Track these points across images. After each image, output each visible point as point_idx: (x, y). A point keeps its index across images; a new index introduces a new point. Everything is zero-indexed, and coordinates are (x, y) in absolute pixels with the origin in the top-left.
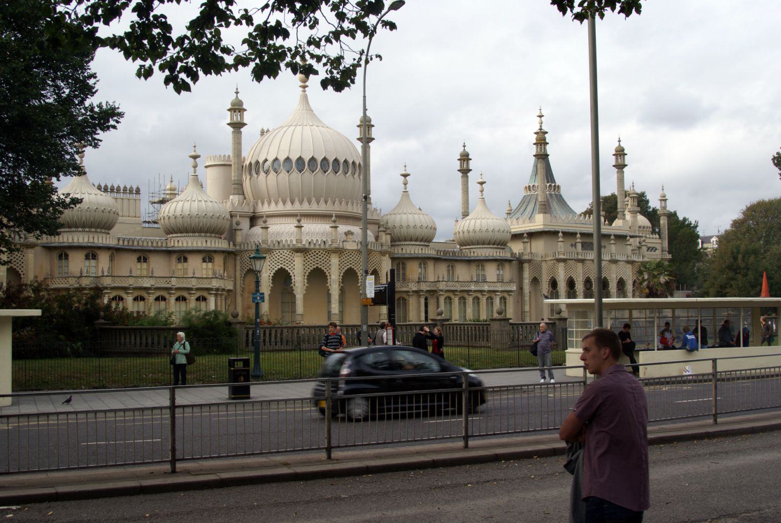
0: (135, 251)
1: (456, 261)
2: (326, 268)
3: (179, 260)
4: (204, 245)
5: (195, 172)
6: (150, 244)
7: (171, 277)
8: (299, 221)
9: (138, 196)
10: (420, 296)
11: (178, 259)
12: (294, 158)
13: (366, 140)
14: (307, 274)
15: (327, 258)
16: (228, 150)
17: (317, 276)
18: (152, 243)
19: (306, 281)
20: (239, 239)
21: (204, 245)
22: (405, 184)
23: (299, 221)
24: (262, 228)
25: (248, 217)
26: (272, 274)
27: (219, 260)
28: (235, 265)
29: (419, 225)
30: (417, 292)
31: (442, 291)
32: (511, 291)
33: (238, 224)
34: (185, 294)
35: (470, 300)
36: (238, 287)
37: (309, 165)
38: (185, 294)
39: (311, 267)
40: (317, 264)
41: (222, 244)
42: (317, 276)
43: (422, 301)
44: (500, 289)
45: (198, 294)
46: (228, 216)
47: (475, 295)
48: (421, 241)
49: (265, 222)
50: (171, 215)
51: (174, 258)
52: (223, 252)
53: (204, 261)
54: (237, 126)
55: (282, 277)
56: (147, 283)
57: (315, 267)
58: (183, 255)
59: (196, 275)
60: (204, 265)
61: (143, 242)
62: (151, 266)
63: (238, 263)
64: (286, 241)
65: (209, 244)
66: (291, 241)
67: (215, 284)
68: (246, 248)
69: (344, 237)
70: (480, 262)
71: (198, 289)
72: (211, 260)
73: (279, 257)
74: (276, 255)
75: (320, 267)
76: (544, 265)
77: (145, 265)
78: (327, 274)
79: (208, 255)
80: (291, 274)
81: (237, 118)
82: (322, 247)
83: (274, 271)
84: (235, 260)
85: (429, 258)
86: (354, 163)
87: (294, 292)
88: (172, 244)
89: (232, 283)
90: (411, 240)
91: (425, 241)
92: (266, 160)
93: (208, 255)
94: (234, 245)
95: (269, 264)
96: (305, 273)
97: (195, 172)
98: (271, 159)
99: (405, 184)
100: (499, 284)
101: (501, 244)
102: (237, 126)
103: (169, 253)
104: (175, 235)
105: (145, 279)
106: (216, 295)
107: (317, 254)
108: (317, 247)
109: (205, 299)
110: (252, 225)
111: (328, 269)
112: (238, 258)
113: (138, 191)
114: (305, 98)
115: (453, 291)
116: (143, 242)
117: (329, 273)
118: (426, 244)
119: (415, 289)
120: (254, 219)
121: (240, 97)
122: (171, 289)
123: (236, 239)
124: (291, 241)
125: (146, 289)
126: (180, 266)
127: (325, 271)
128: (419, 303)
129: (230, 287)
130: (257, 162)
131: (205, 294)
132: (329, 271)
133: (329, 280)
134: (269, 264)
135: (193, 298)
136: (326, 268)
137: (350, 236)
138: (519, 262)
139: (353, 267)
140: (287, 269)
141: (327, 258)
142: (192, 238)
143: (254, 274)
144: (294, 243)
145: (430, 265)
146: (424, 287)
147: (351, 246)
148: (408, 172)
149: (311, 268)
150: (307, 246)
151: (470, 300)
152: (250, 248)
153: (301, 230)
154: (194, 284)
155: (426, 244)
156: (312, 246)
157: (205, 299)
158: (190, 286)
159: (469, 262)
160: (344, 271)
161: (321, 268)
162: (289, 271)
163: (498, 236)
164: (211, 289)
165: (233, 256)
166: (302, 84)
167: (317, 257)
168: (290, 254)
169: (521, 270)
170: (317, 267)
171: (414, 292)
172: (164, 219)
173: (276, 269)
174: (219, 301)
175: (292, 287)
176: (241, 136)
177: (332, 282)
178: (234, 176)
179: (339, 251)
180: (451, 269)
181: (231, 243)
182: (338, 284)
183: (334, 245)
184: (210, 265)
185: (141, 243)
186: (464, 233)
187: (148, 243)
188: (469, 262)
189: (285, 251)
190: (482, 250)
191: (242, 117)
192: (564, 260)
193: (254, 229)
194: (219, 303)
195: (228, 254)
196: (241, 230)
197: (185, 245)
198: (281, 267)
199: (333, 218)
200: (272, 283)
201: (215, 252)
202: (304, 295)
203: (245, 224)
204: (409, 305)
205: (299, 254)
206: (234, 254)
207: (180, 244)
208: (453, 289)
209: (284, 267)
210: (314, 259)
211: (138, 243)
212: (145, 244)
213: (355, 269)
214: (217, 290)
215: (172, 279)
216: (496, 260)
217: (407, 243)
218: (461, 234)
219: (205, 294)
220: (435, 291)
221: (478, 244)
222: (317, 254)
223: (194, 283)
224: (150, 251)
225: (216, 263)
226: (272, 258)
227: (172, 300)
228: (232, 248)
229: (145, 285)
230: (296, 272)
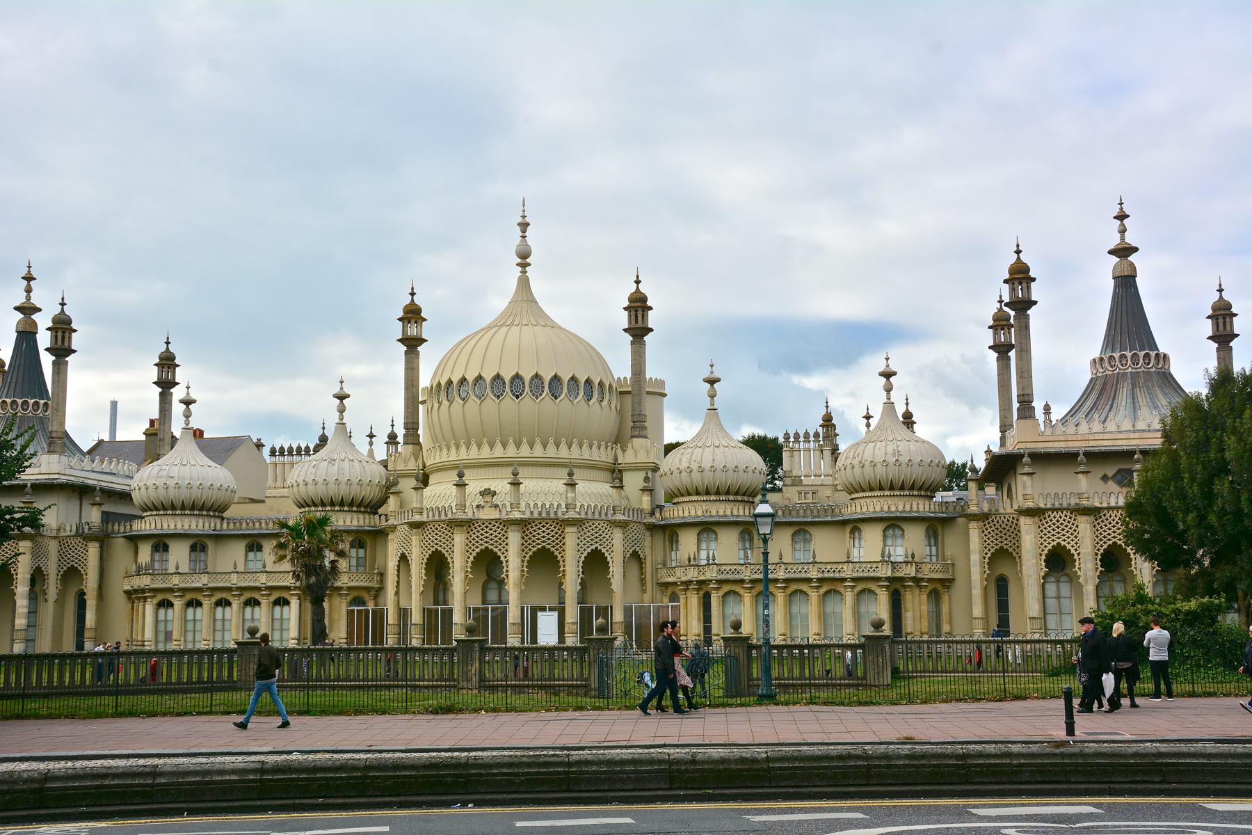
0: (244, 536)
13: (639, 331)
18: (267, 524)
22: (712, 396)
29: (731, 466)
47: (793, 587)
54: (412, 344)
69: (479, 500)
70: (854, 526)
81: (412, 331)
99: (712, 396)
101: (927, 490)
102: (412, 344)
109: (287, 603)
114: (524, 282)
119: (684, 579)
121: (417, 300)
125: (199, 590)
131: (285, 595)
137: (488, 498)
146: (692, 574)
148: (716, 375)
157: (287, 603)
158: (258, 584)
160: (474, 554)
163: (919, 474)
166: (519, 260)
171: (683, 583)
176: (418, 357)
190: (890, 501)
217: (685, 499)
227: (236, 604)
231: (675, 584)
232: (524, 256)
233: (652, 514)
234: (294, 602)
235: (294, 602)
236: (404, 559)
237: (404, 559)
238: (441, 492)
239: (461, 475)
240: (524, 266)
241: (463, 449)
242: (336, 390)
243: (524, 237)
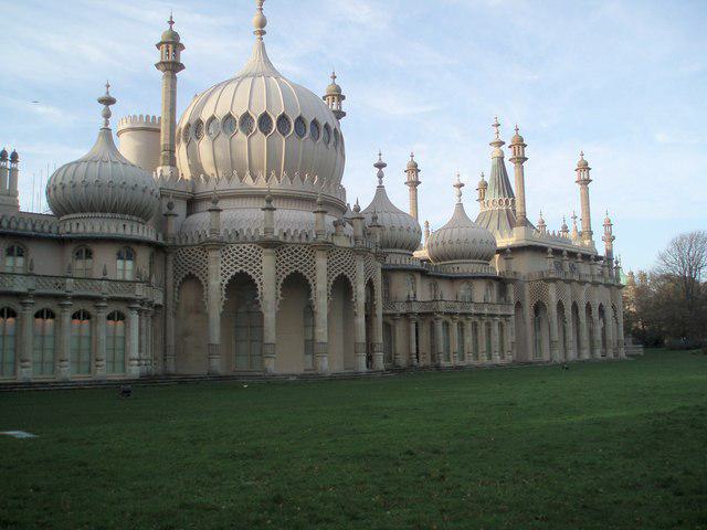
1: (440, 277)
3: (78, 255)
4: (121, 231)
5: (107, 125)
6: (30, 227)
7: (67, 277)
8: (269, 201)
9: (14, 165)
10: (409, 321)
11: (77, 254)
12: (256, 115)
14: (281, 281)
15: (311, 257)
16: (157, 110)
17: (296, 285)
19: (280, 292)
20: (173, 228)
23: (269, 201)
24: (210, 210)
25: (184, 199)
26: (226, 282)
27: (143, 256)
28: (166, 269)
30: (406, 315)
31: (439, 313)
32: (510, 316)
33: (170, 206)
34: (88, 307)
35: (469, 326)
36: (170, 303)
37: (278, 125)
38: (88, 307)
41: (147, 232)
42: (296, 285)
43: (413, 326)
44: (500, 312)
45: (113, 308)
46: (157, 191)
48: (401, 248)
49: (215, 202)
50: (67, 182)
51: (70, 250)
52: (149, 244)
53: (120, 257)
54: (172, 67)
55: (242, 286)
56: (20, 286)
58: (84, 246)
59: (108, 277)
60: (120, 262)
61: (17, 223)
62: (29, 259)
63: (170, 267)
64: (249, 230)
65: (128, 232)
66: (257, 230)
67: (140, 292)
68: (184, 243)
71: (112, 300)
72: (130, 256)
74: (233, 252)
76: (527, 286)
77: (20, 261)
78: (311, 281)
79: (127, 247)
80: (257, 281)
82: (304, 240)
83: (229, 277)
84: (166, 259)
85: (417, 271)
87: (262, 309)
88: (68, 230)
89: (161, 295)
90: (395, 247)
92: (213, 118)
93: (127, 247)
94: (165, 239)
95: (221, 265)
97: (107, 125)
98: (220, 114)
99: (380, 176)
100: (499, 307)
103: (61, 242)
104: (72, 216)
105: (18, 277)
106: (140, 312)
107: (296, 251)
108: (297, 240)
110: (190, 211)
112: (171, 258)
113: (14, 157)
115: (451, 314)
116: (17, 223)
118: (408, 252)
119: (404, 311)
120: (192, 203)
121: (175, 28)
122: (64, 297)
123: (167, 229)
124: (257, 230)
125: (18, 295)
126: (79, 264)
127: (308, 277)
128: (409, 330)
129: (159, 301)
130: (199, 122)
133: (313, 292)
134: (221, 265)
135: (103, 314)
138: (502, 283)
140: (250, 273)
141: (311, 257)
142: (101, 221)
143: (193, 280)
144: (262, 233)
145: (418, 277)
147: (341, 242)
148: (384, 161)
149: (288, 273)
150: (281, 238)
151: (469, 326)
152: (189, 242)
153: (272, 214)
154: (105, 290)
155: (408, 252)
156: (289, 240)
157: (121, 317)
159: (452, 279)
162: (254, 277)
164: (134, 301)
165: (162, 255)
168: (255, 251)
169: (503, 291)
171: (402, 315)
172: (55, 189)
173: (233, 273)
174: (144, 321)
175: (258, 302)
177: (318, 294)
178: (163, 139)
179: (328, 247)
180: (434, 287)
181: (160, 235)
182: (326, 297)
183: (321, 239)
184: (129, 264)
185: (13, 224)
187: (26, 225)
188: (452, 279)
189: (247, 246)
191: (176, 54)
192: (554, 280)
193: (191, 217)
194: (144, 325)
195: (157, 249)
196: (176, 215)
197: (89, 229)
198: (241, 271)
201: (139, 242)
202: (277, 314)
203: (180, 208)
204: (395, 333)
205: (269, 250)
206: (165, 252)
207: (81, 229)
208: (452, 311)
211: (9, 223)
212: (21, 227)
214: (142, 302)
215: (68, 280)
216: (485, 278)
218: (440, 245)
219: (122, 308)
220: (431, 314)
221: (463, 258)
222: (296, 251)
223: (105, 290)
224: (29, 238)
225: (138, 262)
226: (226, 257)
227: (67, 318)
228: (161, 240)
229: (16, 289)
230: (263, 278)
231: (394, 315)
232: (263, 23)
234: (134, 318)
235: (134, 318)
240: (262, 33)
242: (103, 94)
243: (261, 9)
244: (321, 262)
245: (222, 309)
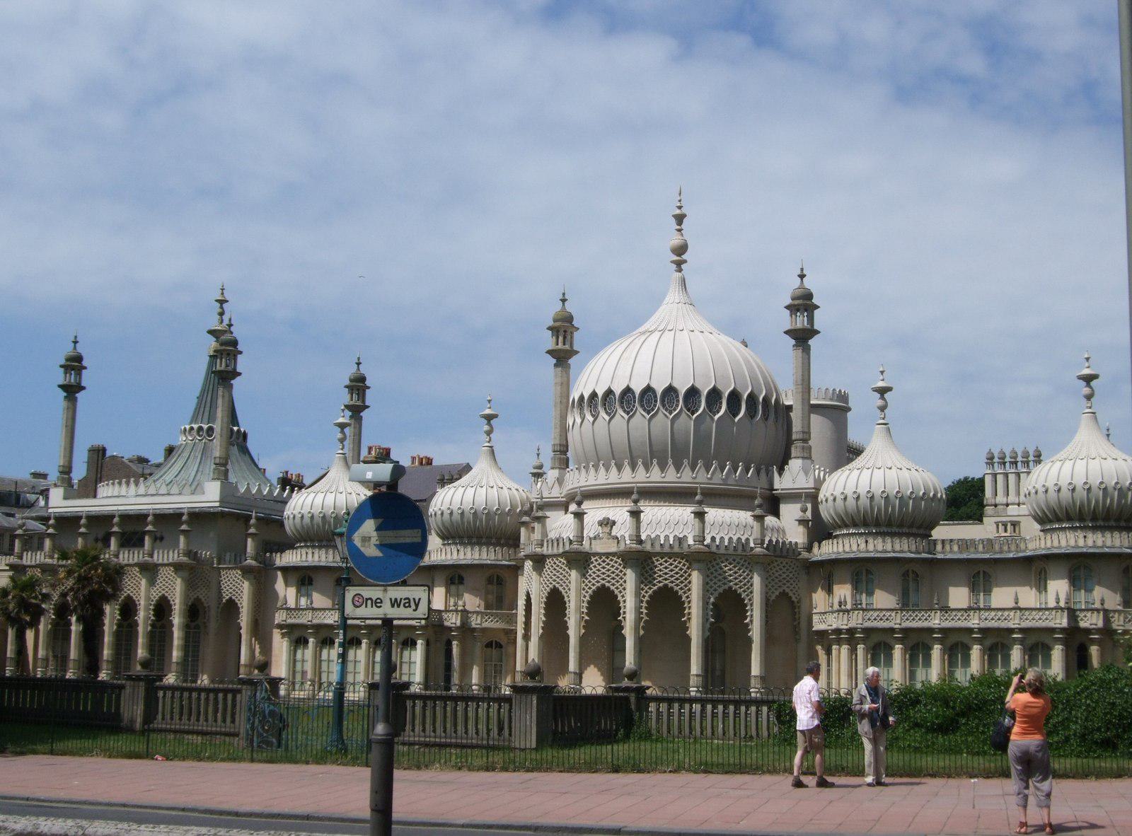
1: (996, 561)
2: (617, 588)
21: (449, 557)
39: (593, 585)
40: (603, 579)
57: (599, 585)
73: (603, 571)
75: (607, 584)
78: (619, 598)
80: (566, 599)
86: (752, 398)
91: (919, 527)
96: (585, 597)
111: (621, 588)
117: (623, 596)
127: (616, 592)
132: (624, 592)
136: (617, 588)
139: (670, 585)
140: (561, 588)
149: (594, 588)
155: (921, 531)
161: (609, 588)
167: (604, 568)
170: (603, 585)
186: (845, 499)
199: (698, 498)
200: (545, 615)
209: (557, 585)
210: (599, 570)
213: (676, 588)
233: (809, 548)
236: (528, 596)
237: (528, 596)
238: (561, 525)
239: (636, 502)
241: (627, 469)
244: (630, 576)
245: (541, 631)
